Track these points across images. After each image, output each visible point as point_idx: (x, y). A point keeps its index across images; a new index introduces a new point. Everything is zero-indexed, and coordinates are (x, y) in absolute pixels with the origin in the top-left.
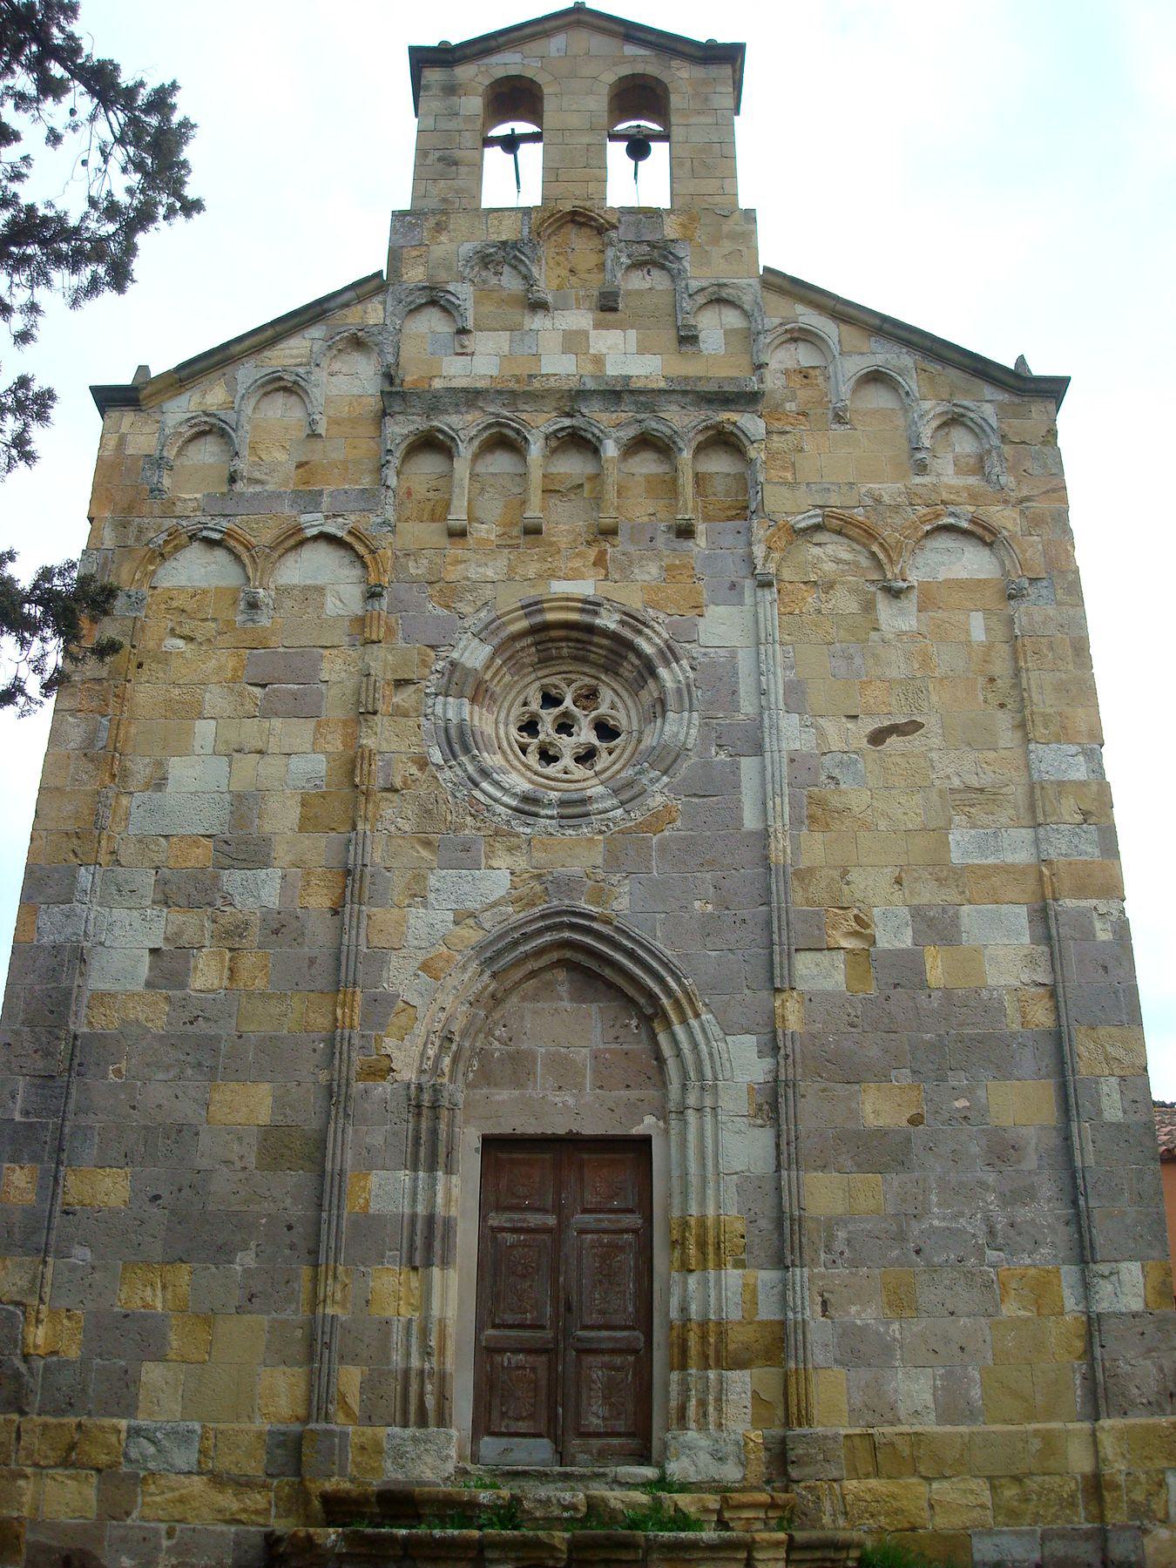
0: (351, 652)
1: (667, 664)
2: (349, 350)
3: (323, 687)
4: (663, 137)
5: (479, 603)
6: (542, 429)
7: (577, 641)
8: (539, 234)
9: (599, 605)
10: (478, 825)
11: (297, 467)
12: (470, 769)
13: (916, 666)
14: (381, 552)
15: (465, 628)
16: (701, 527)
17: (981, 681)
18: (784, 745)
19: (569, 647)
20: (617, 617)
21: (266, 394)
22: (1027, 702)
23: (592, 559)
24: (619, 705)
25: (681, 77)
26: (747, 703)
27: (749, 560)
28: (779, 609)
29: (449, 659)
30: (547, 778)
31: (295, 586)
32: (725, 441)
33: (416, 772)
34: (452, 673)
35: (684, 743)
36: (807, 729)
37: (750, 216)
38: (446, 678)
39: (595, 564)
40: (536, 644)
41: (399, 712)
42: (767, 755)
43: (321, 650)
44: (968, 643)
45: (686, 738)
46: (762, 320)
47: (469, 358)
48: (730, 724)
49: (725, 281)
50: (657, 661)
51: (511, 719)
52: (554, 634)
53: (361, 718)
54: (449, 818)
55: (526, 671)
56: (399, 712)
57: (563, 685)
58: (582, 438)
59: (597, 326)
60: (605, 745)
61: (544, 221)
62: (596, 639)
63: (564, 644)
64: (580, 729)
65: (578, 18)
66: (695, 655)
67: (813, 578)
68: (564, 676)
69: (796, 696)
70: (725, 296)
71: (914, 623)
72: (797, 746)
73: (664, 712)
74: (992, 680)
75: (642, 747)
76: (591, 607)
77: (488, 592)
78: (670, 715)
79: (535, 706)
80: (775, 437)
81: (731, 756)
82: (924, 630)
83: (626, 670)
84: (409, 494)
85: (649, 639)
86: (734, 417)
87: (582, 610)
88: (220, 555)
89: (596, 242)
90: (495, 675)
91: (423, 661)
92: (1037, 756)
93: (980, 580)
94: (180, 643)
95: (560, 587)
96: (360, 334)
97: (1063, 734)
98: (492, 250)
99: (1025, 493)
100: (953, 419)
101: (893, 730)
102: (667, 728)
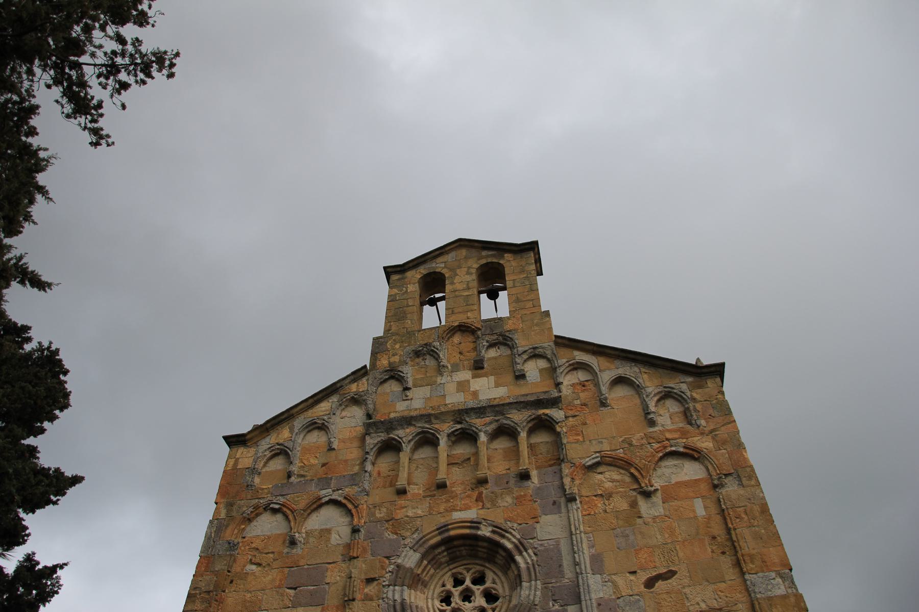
0: (343, 565)
1: (521, 553)
2: (351, 405)
3: (327, 586)
4: (504, 289)
5: (413, 530)
6: (446, 431)
7: (470, 545)
8: (443, 338)
9: (480, 523)
11: (322, 466)
13: (667, 536)
14: (361, 506)
15: (406, 545)
16: (534, 474)
17: (707, 540)
18: (593, 596)
19: (466, 550)
20: (490, 529)
21: (309, 432)
22: (738, 548)
23: (475, 498)
24: (497, 581)
25: (509, 262)
26: (568, 572)
27: (562, 487)
28: (582, 513)
29: (396, 564)
31: (316, 530)
32: (544, 425)
34: (398, 571)
35: (534, 601)
36: (606, 584)
37: (547, 314)
38: (394, 575)
39: (477, 500)
40: (446, 550)
41: (368, 598)
42: (583, 603)
43: (327, 565)
44: (695, 517)
45: (534, 598)
46: (557, 361)
47: (410, 401)
48: (560, 586)
49: (536, 345)
50: (515, 552)
51: (435, 595)
52: (456, 543)
53: (346, 603)
55: (443, 566)
56: (368, 598)
57: (465, 572)
58: (468, 434)
59: (474, 377)
60: (490, 606)
61: (445, 331)
62: (480, 543)
63: (462, 548)
64: (475, 598)
65: (461, 243)
66: (536, 546)
67: (599, 492)
68: (465, 567)
69: (598, 563)
70: (537, 353)
71: (662, 510)
72: (601, 595)
73: (521, 582)
74: (714, 538)
75: (511, 605)
76: (475, 525)
77: (418, 522)
78: (524, 584)
79: (449, 586)
80: (571, 419)
81: (562, 606)
82: (667, 513)
83: (500, 560)
84: (379, 474)
85: (509, 540)
86: (547, 411)
88: (279, 517)
89: (471, 338)
90: (423, 570)
91: (382, 566)
92: (751, 583)
93: (696, 480)
94: (254, 567)
95: (457, 516)
96: (355, 397)
97: (765, 566)
98: (421, 348)
99: (712, 427)
100: (665, 395)
101: (660, 577)
102: (522, 592)
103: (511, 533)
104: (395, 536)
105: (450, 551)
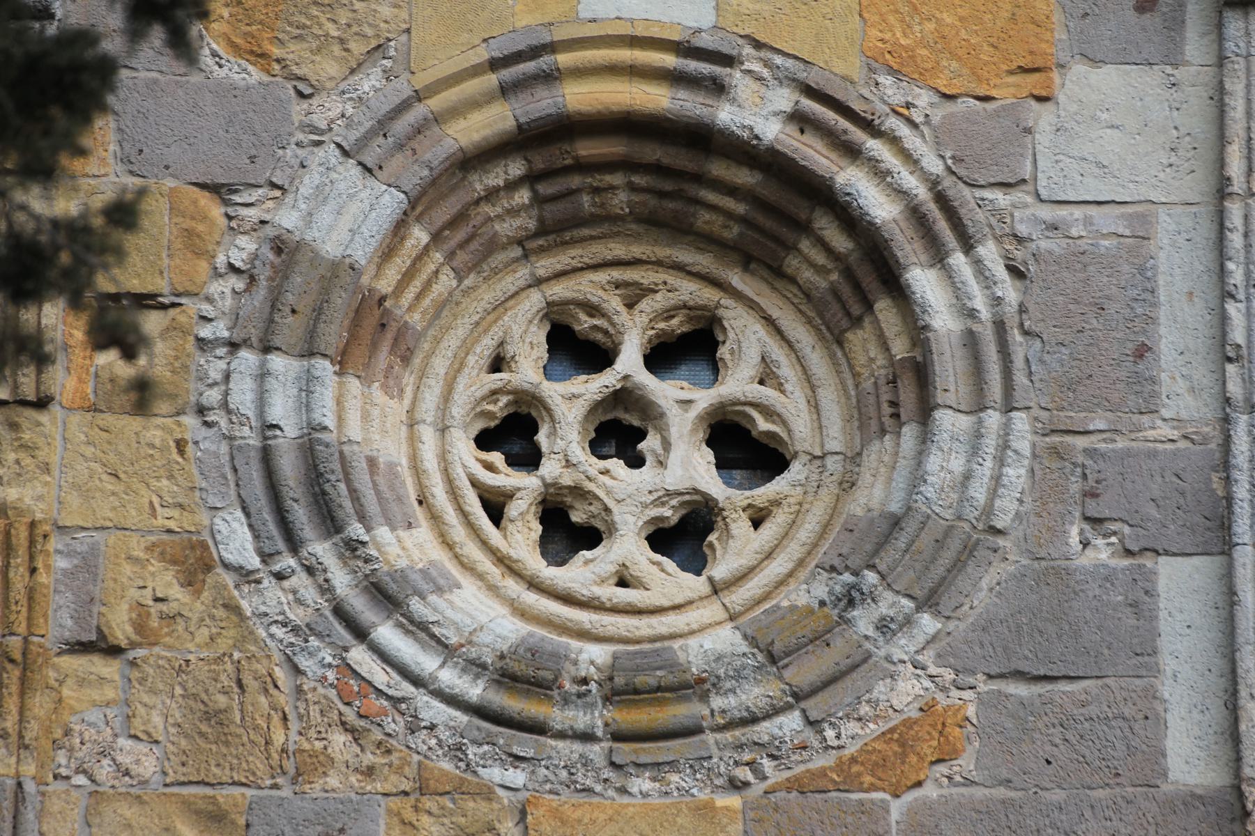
5: (358, 48)
9: (728, 61)
10: (369, 758)
12: (341, 580)
20: (785, 99)
30: (568, 599)
33: (177, 593)
34: (282, 274)
38: (261, 292)
40: (531, 179)
52: (587, 149)
54: (279, 737)
62: (719, 169)
85: (880, 174)
87: (676, 78)
103: (894, 141)
104: (256, 75)
105: (545, 189)
